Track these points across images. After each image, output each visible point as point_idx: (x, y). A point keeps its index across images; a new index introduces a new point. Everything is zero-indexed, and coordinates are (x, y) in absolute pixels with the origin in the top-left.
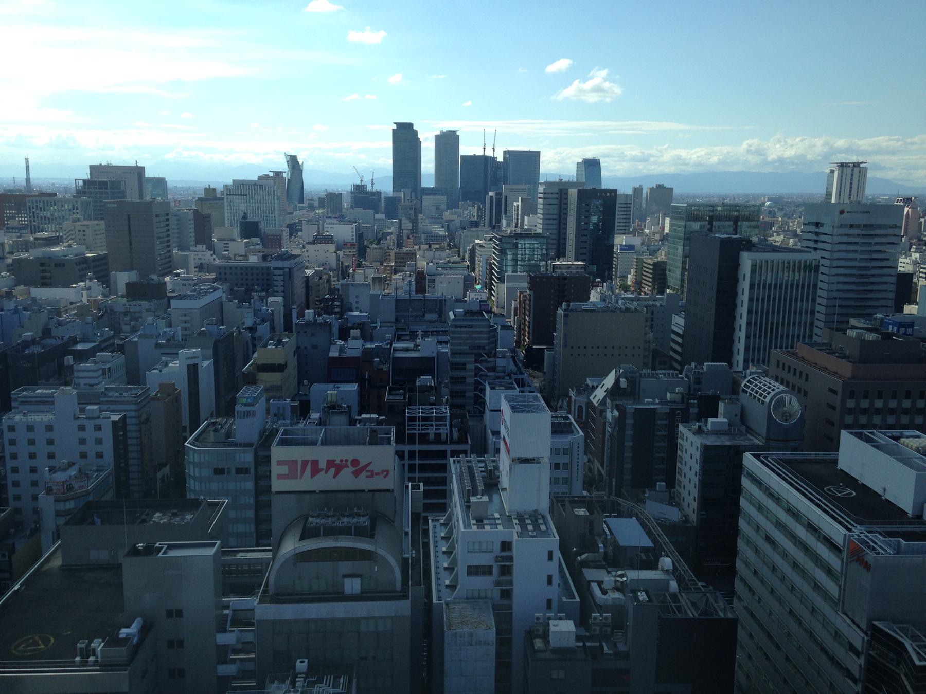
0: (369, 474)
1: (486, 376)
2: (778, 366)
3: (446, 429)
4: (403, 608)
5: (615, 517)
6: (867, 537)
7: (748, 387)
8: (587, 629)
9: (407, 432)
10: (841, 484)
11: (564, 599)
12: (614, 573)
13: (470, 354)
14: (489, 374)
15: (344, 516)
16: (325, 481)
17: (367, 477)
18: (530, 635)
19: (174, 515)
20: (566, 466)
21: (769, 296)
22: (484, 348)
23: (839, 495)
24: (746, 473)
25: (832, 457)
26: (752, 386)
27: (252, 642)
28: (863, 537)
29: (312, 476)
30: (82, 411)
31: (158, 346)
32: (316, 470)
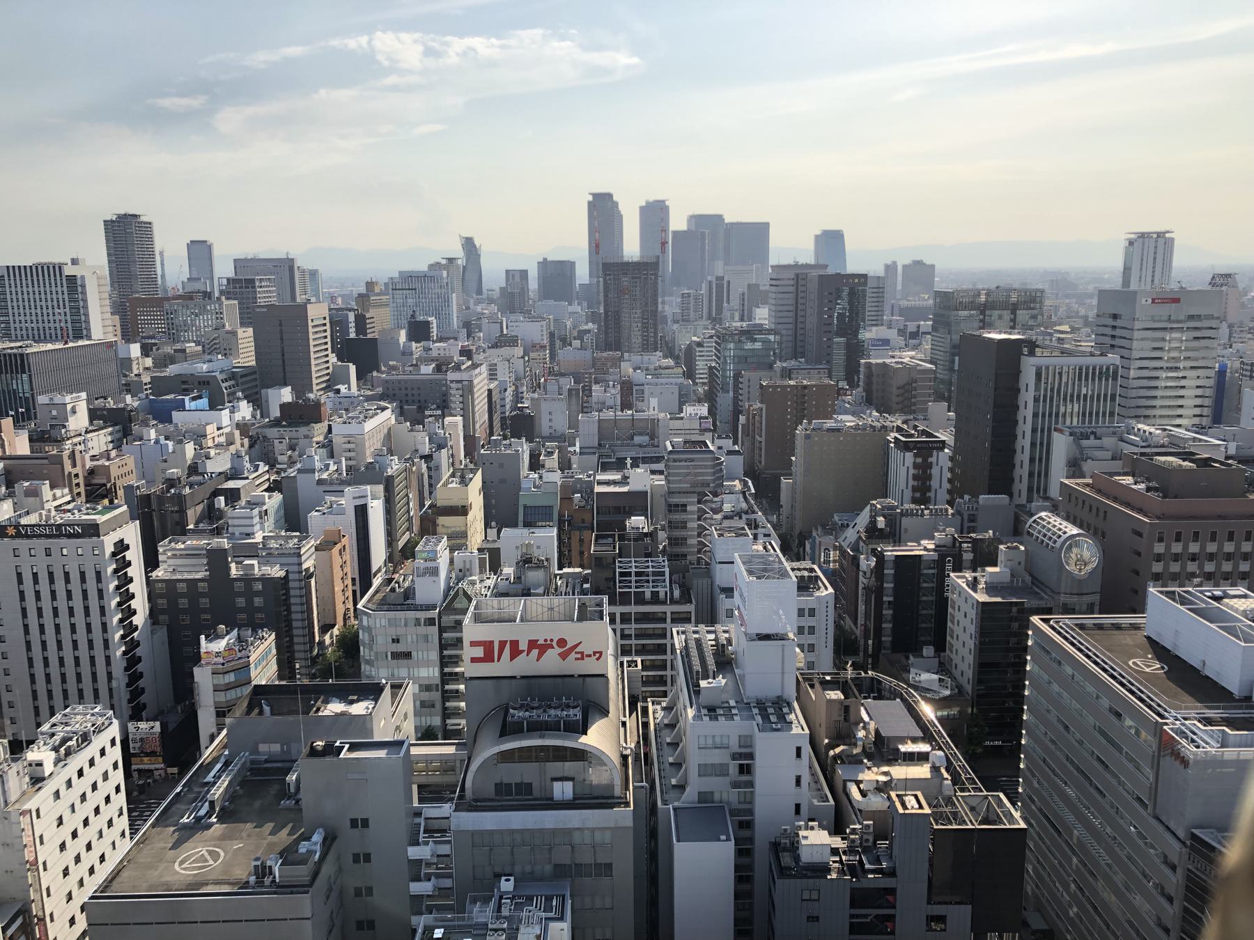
0: (579, 656)
3: (665, 587)
4: (623, 816)
5: (875, 698)
7: (1035, 529)
8: (843, 839)
10: (1150, 656)
11: (815, 802)
12: (875, 769)
13: (691, 493)
15: (550, 707)
17: (577, 659)
18: (776, 847)
19: (352, 702)
23: (1148, 670)
27: (448, 856)
29: (512, 659)
32: (515, 652)
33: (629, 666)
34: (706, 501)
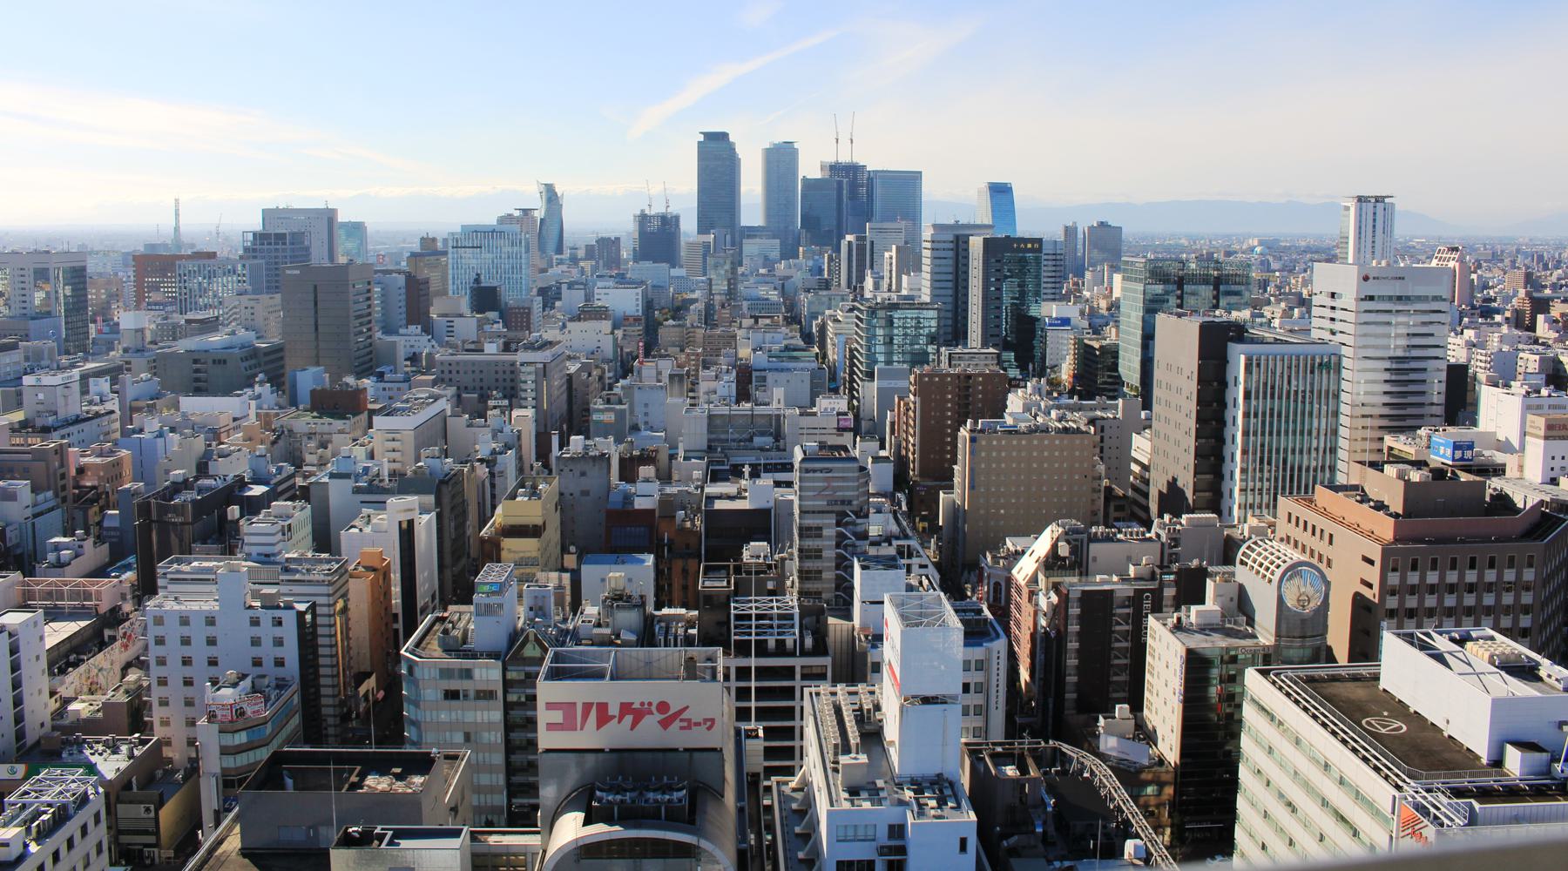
0: (685, 724)
1: (854, 546)
2: (1289, 521)
3: (794, 634)
6: (1424, 798)
7: (1248, 557)
9: (734, 638)
10: (1386, 714)
15: (648, 790)
16: (616, 735)
20: (980, 688)
21: (1272, 410)
22: (850, 503)
24: (1249, 698)
25: (1373, 670)
26: (1253, 555)
28: (1420, 799)
29: (599, 726)
32: (603, 718)
34: (847, 524)
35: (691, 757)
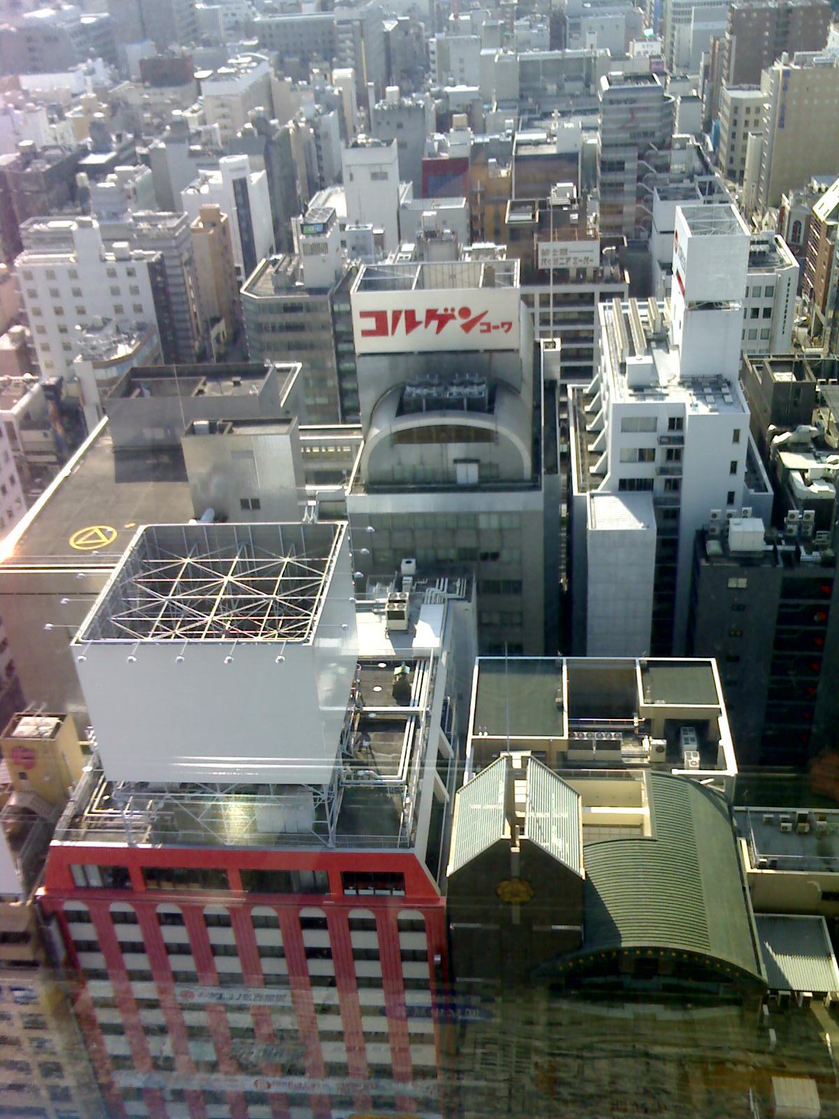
1: (655, 179)
5: (833, 383)
14: (661, 176)
15: (452, 384)
16: (425, 338)
17: (482, 331)
18: (702, 536)
22: (653, 134)
30: (110, 249)
31: (193, 154)
32: (412, 323)
33: (546, 347)
35: (491, 358)
